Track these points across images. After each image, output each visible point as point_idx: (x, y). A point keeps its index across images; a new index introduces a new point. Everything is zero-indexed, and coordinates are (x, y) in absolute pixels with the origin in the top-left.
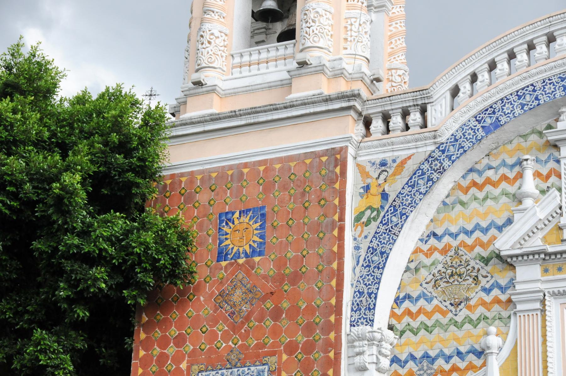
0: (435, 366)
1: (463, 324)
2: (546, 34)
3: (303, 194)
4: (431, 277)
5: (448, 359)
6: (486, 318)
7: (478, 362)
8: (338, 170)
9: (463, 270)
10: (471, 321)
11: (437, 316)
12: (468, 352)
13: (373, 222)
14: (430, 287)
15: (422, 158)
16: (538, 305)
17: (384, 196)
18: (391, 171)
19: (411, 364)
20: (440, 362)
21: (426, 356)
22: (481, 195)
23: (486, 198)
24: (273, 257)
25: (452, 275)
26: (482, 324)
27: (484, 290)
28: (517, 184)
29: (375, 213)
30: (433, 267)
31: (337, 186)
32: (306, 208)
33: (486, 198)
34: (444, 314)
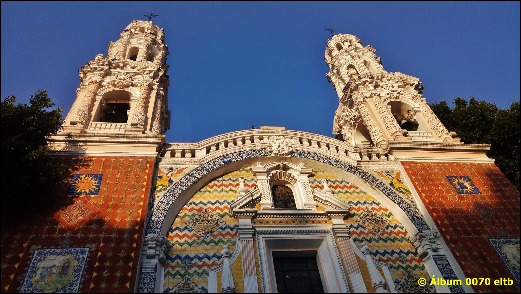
0: (193, 261)
1: (210, 243)
2: (250, 136)
3: (126, 172)
4: (192, 220)
5: (200, 259)
6: (222, 241)
7: (219, 262)
8: (148, 165)
9: (209, 219)
10: (214, 242)
11: (195, 238)
12: (213, 257)
13: (163, 191)
14: (190, 225)
15: (192, 169)
16: (251, 236)
17: (171, 181)
18: (175, 172)
19: (178, 261)
20: (196, 260)
21: (187, 257)
22: (220, 190)
23: (222, 191)
24: (103, 196)
25: (203, 221)
26: (221, 244)
27: (221, 228)
28: (237, 187)
29: (165, 187)
30: (192, 217)
31: (147, 171)
32: (128, 178)
33: (222, 191)
34: (199, 237)
